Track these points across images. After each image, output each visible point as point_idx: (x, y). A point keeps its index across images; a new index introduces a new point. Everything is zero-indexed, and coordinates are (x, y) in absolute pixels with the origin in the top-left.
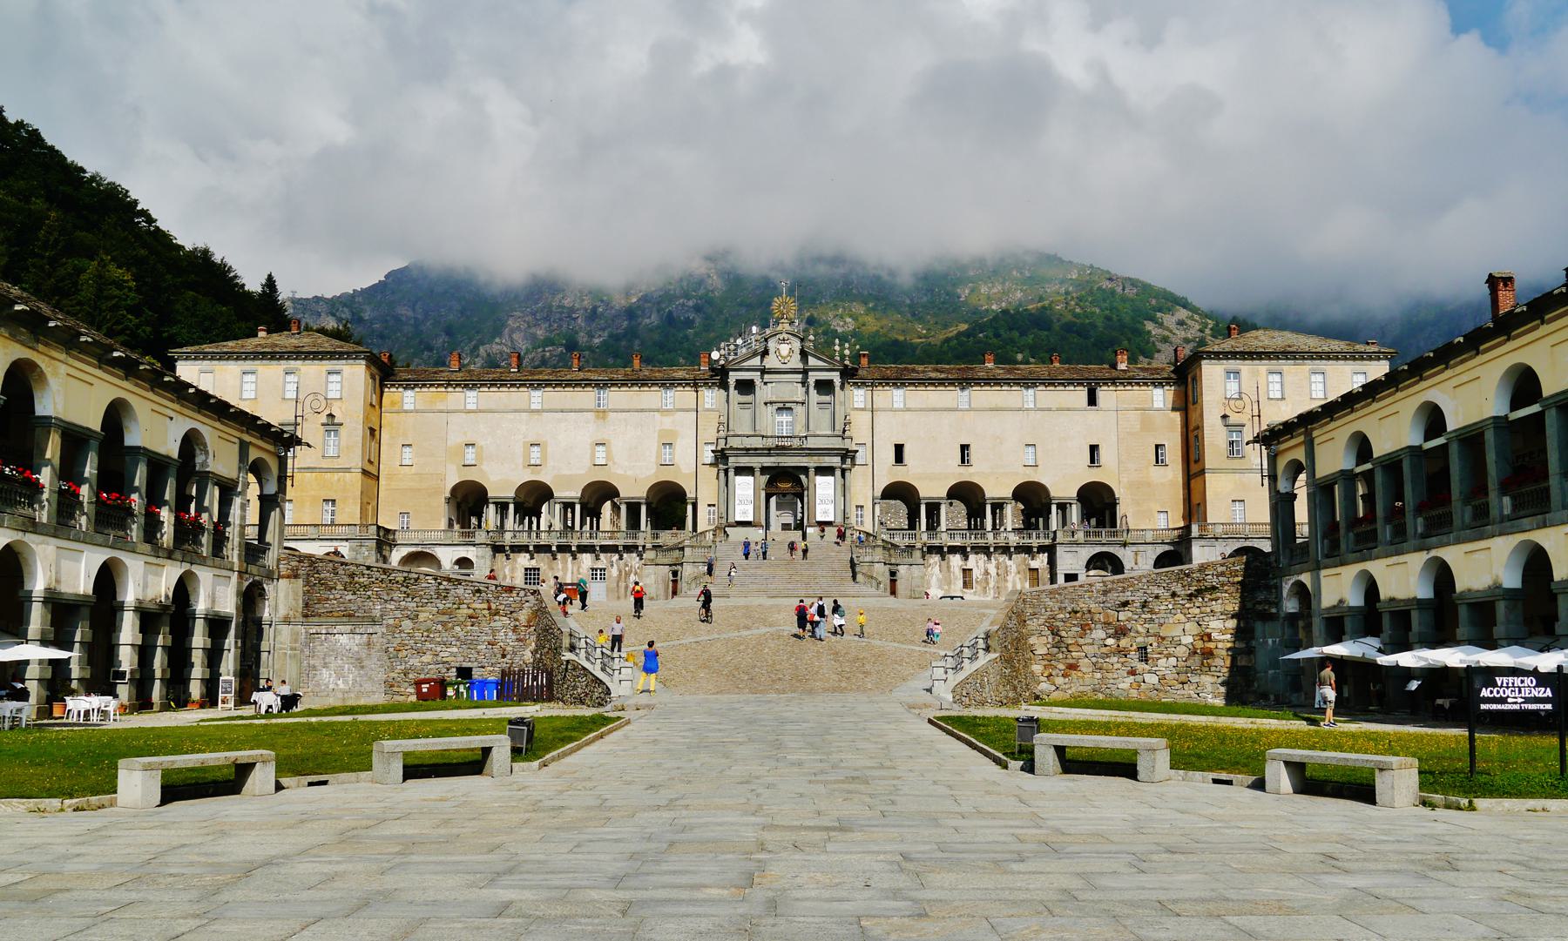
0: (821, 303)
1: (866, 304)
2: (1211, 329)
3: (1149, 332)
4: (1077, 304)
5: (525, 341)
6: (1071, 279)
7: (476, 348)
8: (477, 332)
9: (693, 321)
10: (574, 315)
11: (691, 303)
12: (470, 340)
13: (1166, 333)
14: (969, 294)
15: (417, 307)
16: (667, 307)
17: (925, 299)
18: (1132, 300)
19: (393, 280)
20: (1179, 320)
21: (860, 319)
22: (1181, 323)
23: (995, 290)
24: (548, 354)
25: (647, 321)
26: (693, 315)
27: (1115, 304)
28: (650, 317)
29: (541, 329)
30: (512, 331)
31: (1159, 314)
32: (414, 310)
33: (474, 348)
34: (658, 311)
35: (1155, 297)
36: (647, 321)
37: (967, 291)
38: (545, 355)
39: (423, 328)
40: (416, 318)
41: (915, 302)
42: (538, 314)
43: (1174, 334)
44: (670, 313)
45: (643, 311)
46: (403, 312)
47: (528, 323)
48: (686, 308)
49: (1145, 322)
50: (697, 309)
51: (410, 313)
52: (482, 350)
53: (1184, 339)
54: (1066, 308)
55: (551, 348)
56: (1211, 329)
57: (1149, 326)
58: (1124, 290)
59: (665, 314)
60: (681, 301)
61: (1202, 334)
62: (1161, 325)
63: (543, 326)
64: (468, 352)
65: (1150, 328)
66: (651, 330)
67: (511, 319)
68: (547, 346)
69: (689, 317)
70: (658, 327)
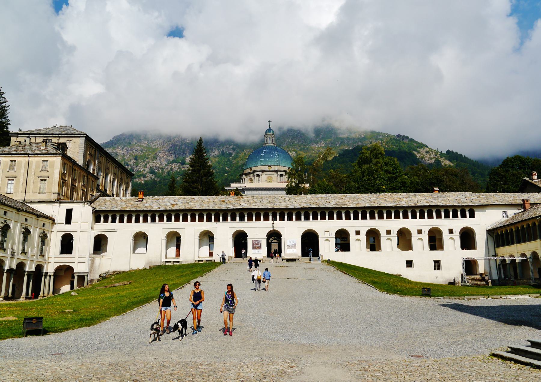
0: (282, 146)
1: (300, 147)
2: (439, 155)
3: (416, 155)
4: (386, 144)
5: (166, 162)
6: (380, 138)
7: (146, 164)
8: (147, 159)
9: (232, 154)
10: (185, 152)
11: (231, 147)
12: (144, 161)
13: (422, 155)
14: (340, 144)
15: (124, 149)
16: (221, 149)
17: (323, 145)
18: (407, 144)
19: (115, 140)
20: (426, 151)
21: (298, 152)
22: (427, 152)
23: (350, 142)
24: (174, 166)
25: (214, 154)
26: (232, 152)
27: (401, 145)
28: (215, 152)
29: (172, 157)
30: (160, 158)
31: (418, 149)
32: (123, 150)
33: (145, 165)
34: (218, 150)
35: (415, 143)
36: (214, 154)
37: (339, 143)
38: (172, 167)
39: (126, 157)
40: (123, 154)
41: (320, 146)
42: (171, 152)
43: (425, 156)
44: (223, 151)
45: (212, 150)
46: (118, 151)
47: (167, 155)
48: (229, 149)
49: (413, 152)
50: (234, 149)
51: (121, 152)
52: (148, 165)
53: (429, 158)
54: (382, 146)
55: (175, 164)
56: (439, 155)
57: (415, 153)
58: (403, 140)
59: (221, 151)
60: (227, 146)
61: (436, 156)
62: (419, 153)
63: (173, 156)
64: (143, 166)
65: (415, 154)
66: (215, 157)
67: (160, 153)
68: (173, 163)
69: (230, 153)
70: (218, 156)
